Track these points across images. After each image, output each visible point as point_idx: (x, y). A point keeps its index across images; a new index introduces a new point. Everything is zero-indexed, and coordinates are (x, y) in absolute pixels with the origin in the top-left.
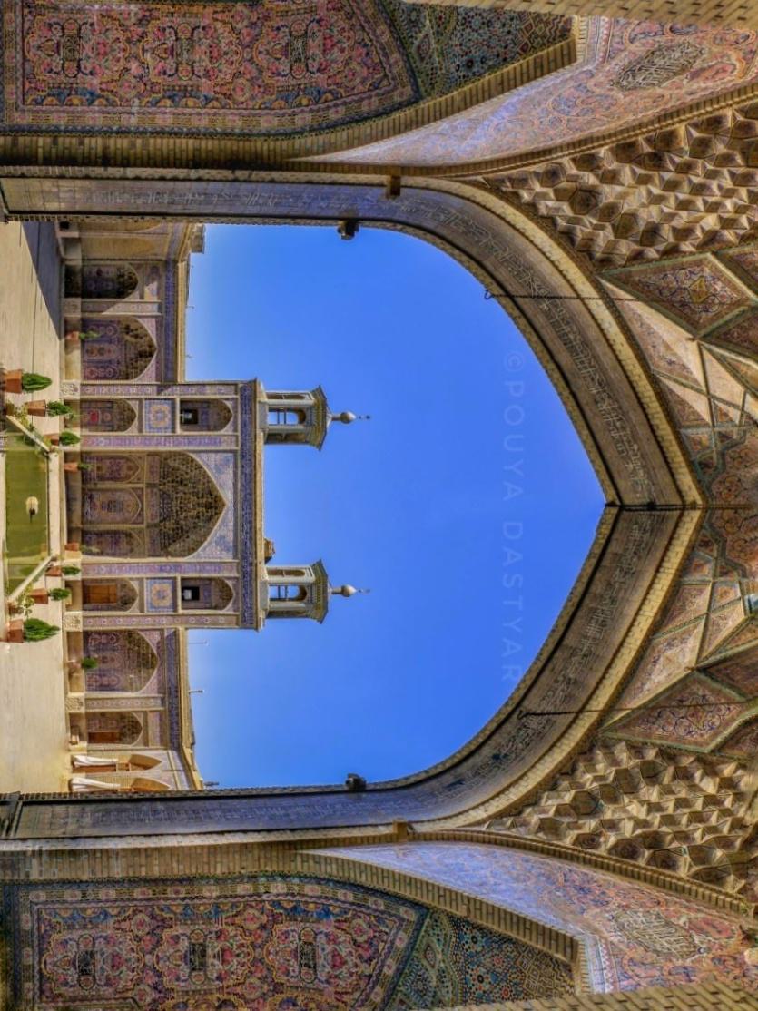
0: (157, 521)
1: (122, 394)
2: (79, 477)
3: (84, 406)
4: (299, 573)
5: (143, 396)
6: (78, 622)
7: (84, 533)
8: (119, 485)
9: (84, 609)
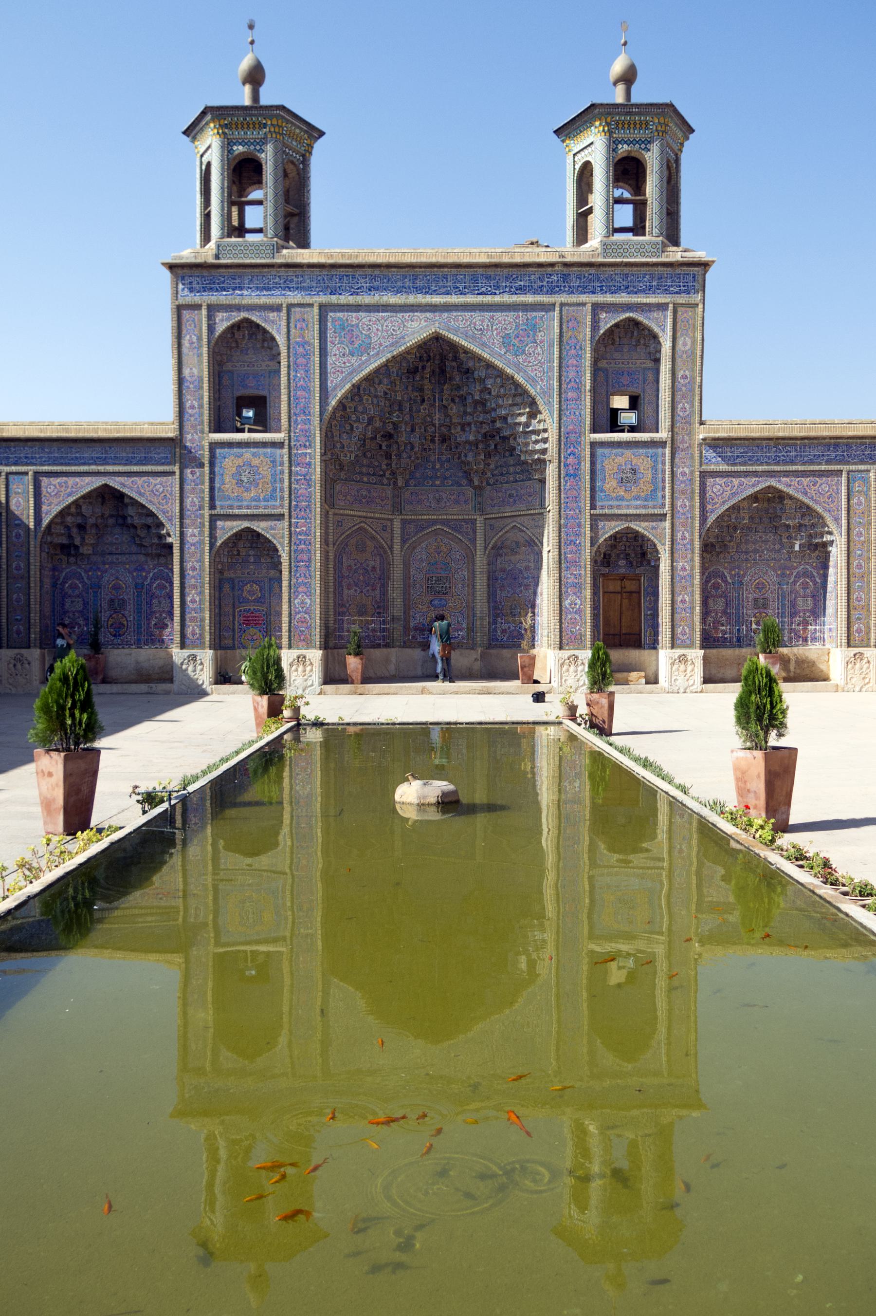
0: (470, 492)
1: (201, 561)
2: (377, 653)
3: (228, 642)
4: (585, 174)
5: (206, 513)
6: (683, 659)
7: (493, 642)
8: (397, 573)
9: (654, 645)
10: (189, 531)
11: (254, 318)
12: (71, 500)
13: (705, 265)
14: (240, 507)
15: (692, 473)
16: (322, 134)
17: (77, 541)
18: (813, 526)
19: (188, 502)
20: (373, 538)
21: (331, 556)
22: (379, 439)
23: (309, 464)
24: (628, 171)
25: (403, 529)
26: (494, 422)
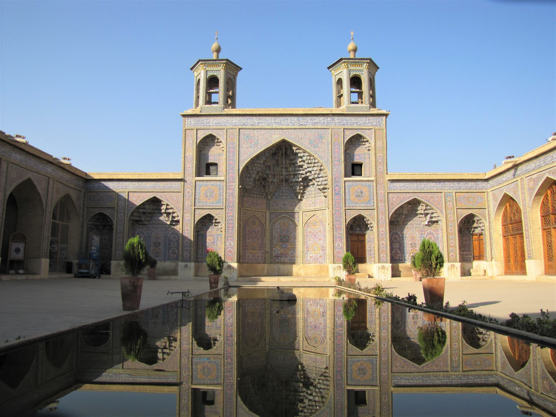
1: (190, 227)
3: (200, 260)
5: (193, 208)
6: (383, 268)
8: (268, 234)
10: (186, 215)
11: (214, 134)
12: (141, 202)
13: (386, 115)
14: (206, 206)
15: (384, 193)
16: (241, 69)
17: (143, 219)
18: (432, 213)
19: (186, 204)
20: (258, 219)
21: (242, 227)
22: (261, 181)
23: (233, 189)
24: (356, 82)
25: (270, 216)
26: (306, 173)
